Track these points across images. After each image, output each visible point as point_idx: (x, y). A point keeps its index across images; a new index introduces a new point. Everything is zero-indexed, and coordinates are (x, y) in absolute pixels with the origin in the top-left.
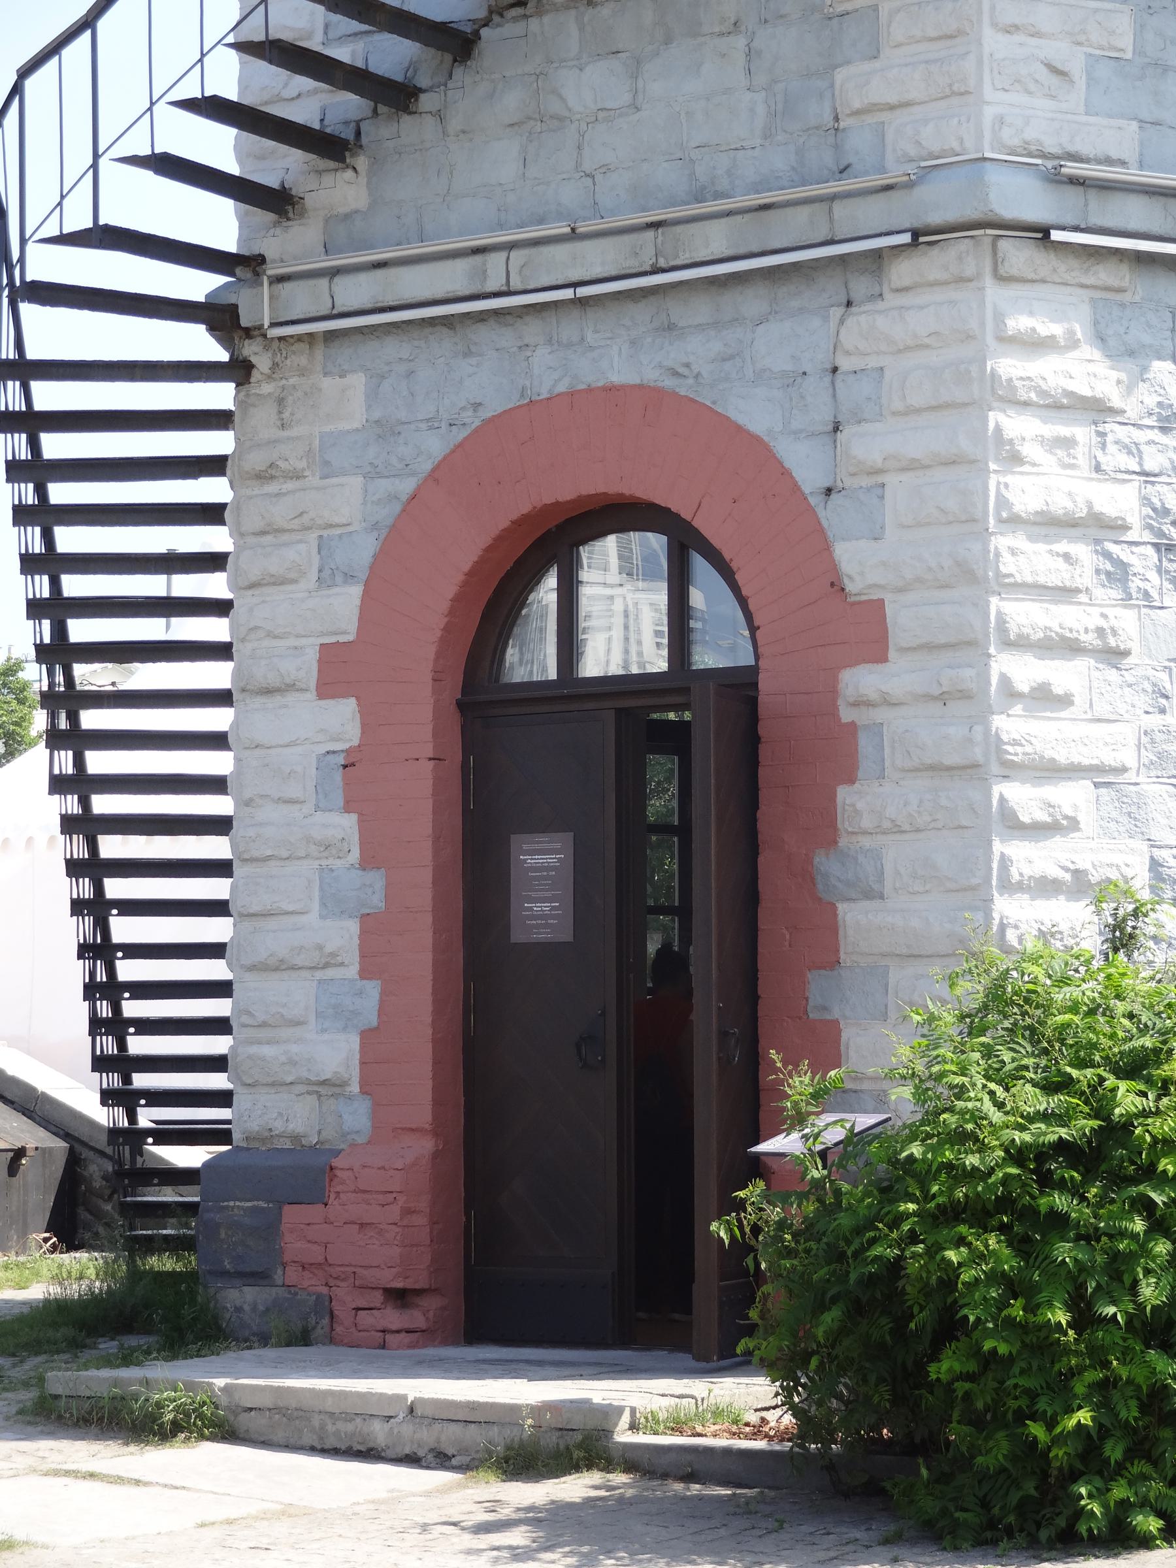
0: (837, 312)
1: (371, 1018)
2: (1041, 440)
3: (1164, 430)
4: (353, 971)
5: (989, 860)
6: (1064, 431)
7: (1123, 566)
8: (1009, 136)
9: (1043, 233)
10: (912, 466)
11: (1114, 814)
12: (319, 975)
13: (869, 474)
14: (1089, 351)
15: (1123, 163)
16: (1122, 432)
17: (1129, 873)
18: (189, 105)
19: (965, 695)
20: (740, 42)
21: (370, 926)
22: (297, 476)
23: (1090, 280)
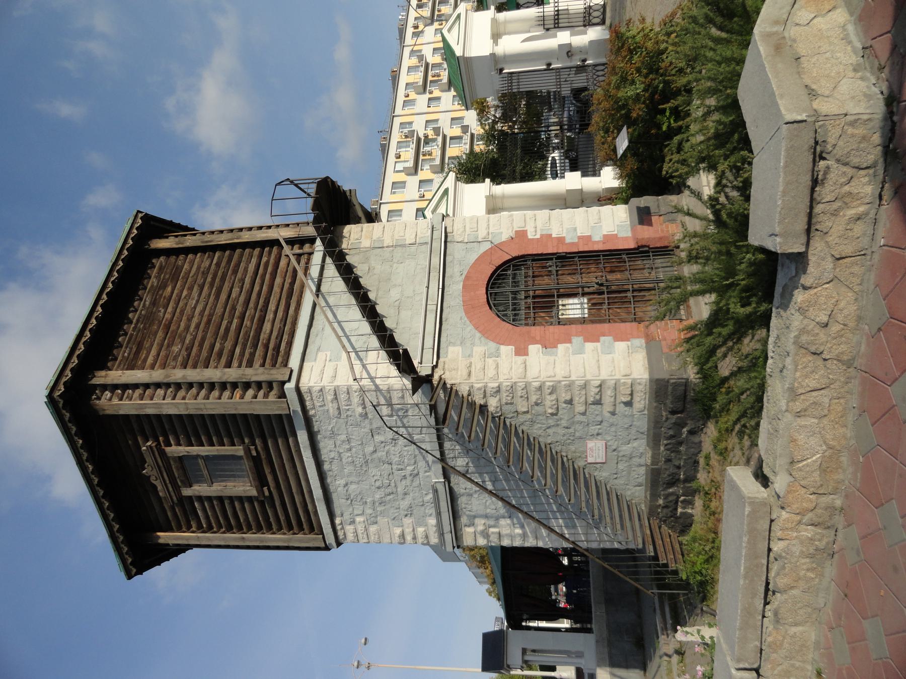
4: (598, 344)
12: (600, 354)
21: (587, 340)
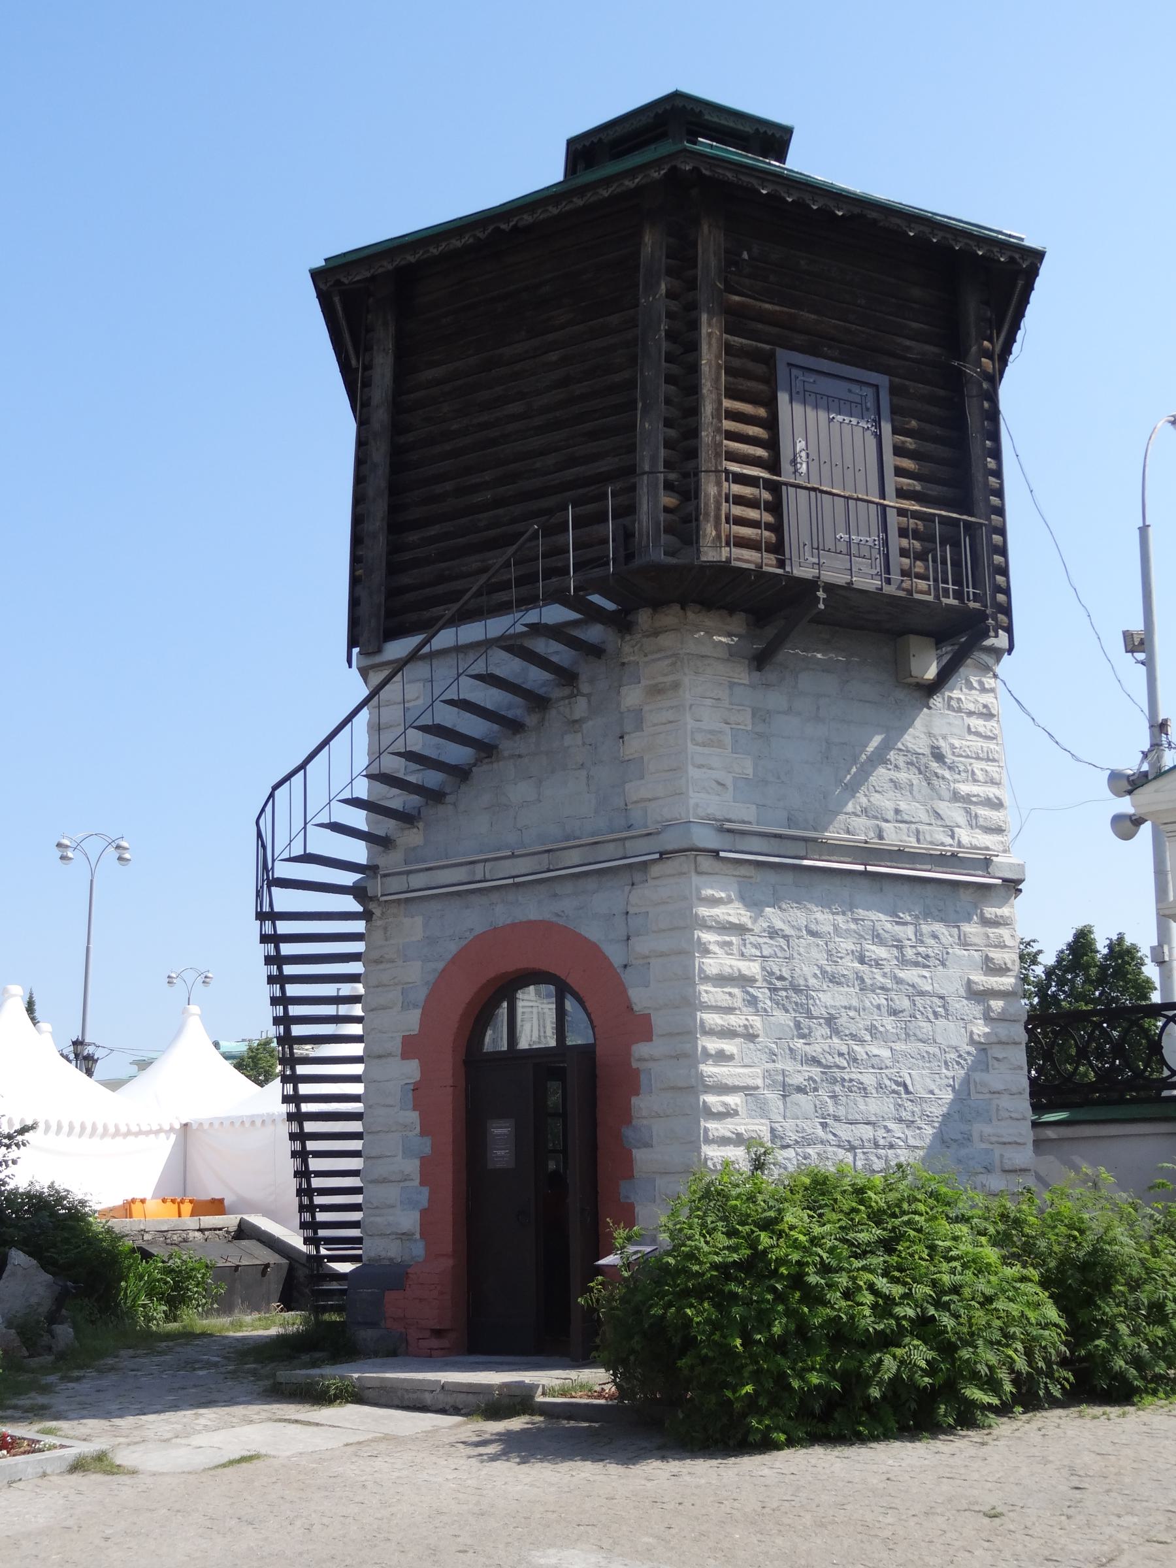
0: (627, 888)
1: (425, 1204)
2: (717, 943)
3: (771, 938)
4: (417, 1182)
5: (699, 1130)
6: (727, 939)
7: (755, 998)
8: (701, 812)
9: (716, 853)
10: (662, 955)
11: (754, 1108)
12: (402, 1184)
13: (643, 958)
14: (737, 904)
15: (750, 823)
16: (752, 939)
17: (762, 1134)
18: (346, 801)
19: (686, 1056)
20: (584, 773)
21: (425, 1162)
22: (393, 961)
23: (737, 873)
